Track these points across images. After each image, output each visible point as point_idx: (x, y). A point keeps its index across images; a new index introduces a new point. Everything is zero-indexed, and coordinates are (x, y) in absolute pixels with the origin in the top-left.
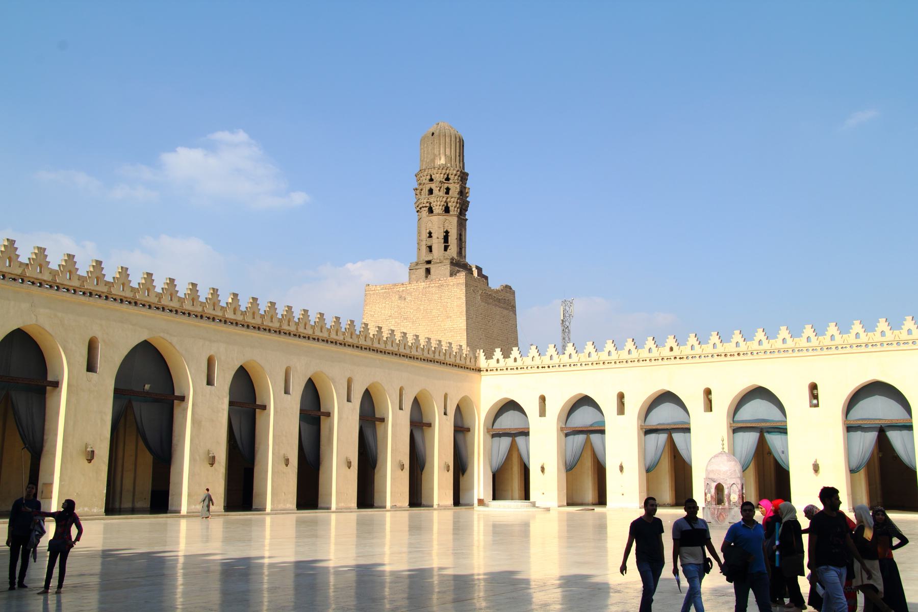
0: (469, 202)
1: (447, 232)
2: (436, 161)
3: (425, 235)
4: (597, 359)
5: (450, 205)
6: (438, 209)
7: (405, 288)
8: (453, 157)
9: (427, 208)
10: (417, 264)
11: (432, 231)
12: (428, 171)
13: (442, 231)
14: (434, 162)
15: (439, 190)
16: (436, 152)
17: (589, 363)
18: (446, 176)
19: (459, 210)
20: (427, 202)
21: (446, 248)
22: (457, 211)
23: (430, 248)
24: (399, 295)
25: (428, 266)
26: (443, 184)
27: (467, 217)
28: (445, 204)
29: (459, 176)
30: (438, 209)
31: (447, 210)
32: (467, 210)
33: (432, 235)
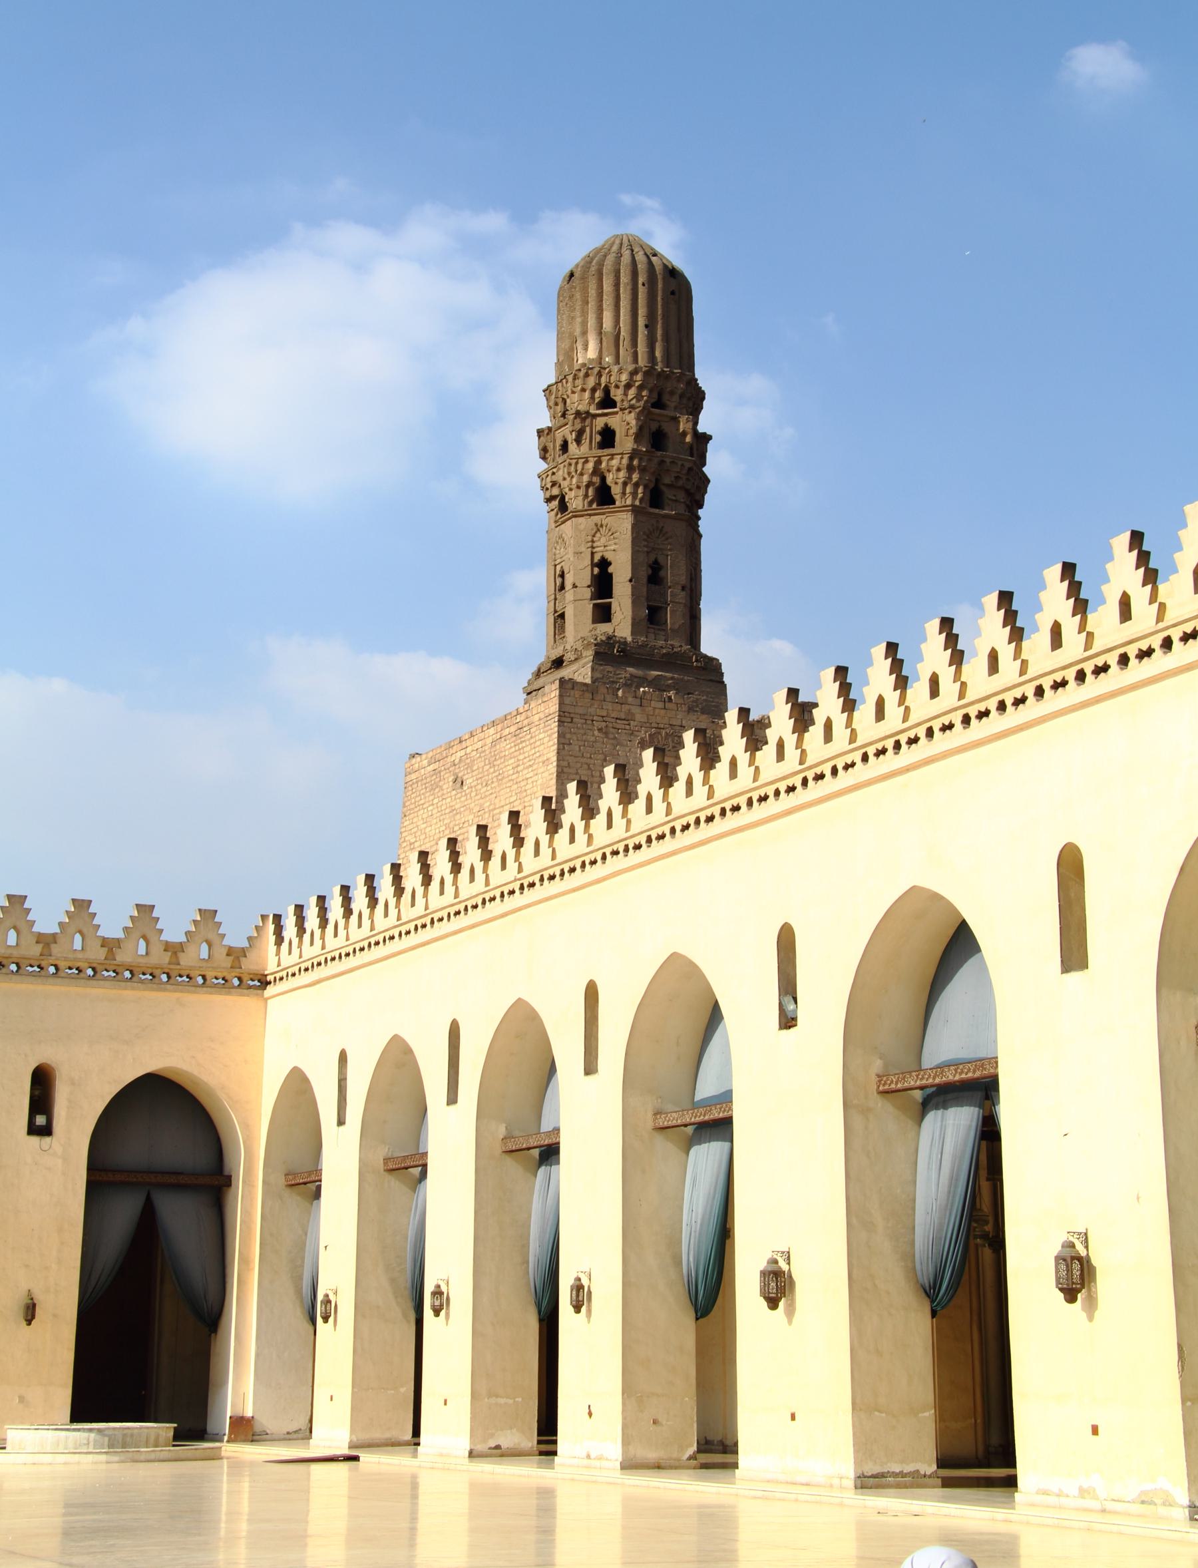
5: (610, 478)
6: (576, 501)
7: (463, 753)
8: (625, 333)
9: (555, 503)
12: (558, 390)
16: (578, 332)
18: (598, 394)
19: (640, 490)
21: (603, 614)
22: (634, 494)
24: (453, 775)
26: (588, 422)
28: (596, 480)
29: (641, 388)
30: (576, 501)
31: (604, 497)
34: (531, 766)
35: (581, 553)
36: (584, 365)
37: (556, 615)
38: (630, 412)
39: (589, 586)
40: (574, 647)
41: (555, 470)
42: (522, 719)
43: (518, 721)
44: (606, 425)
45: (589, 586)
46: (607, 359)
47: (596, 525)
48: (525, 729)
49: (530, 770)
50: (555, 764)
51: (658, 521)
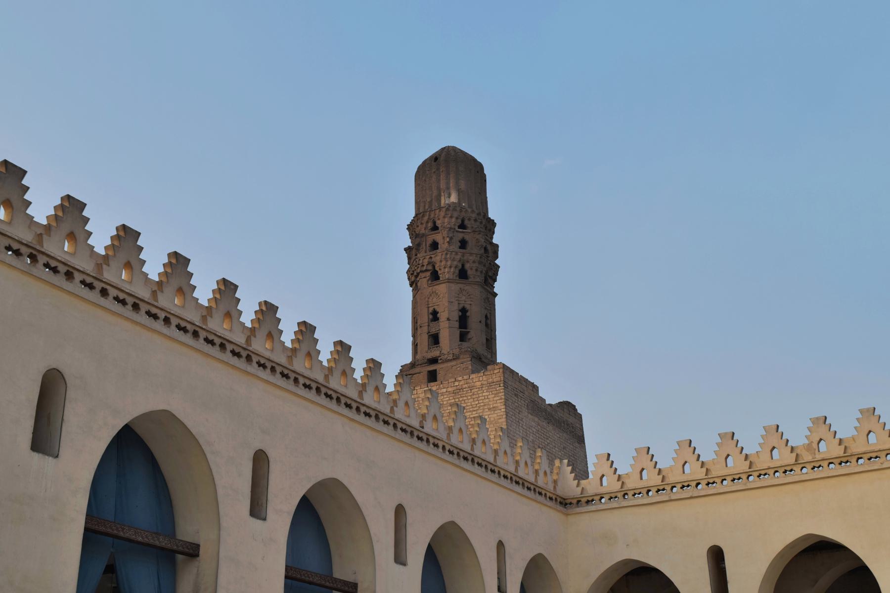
0: (499, 267)
1: (464, 311)
2: (443, 198)
3: (425, 318)
4: (841, 454)
5: (467, 266)
6: (446, 273)
9: (428, 274)
10: (413, 365)
11: (438, 310)
12: (430, 215)
13: (456, 307)
14: (440, 201)
15: (448, 242)
17: (822, 463)
18: (460, 221)
20: (429, 263)
21: (463, 337)
23: (435, 339)
25: (432, 368)
27: (495, 290)
28: (460, 266)
30: (446, 273)
31: (463, 274)
32: (495, 280)
33: (438, 315)
34: (474, 411)
35: (452, 302)
36: (449, 205)
37: (429, 334)
38: (479, 234)
39: (457, 321)
40: (451, 352)
41: (433, 256)
42: (460, 384)
43: (455, 385)
44: (463, 238)
45: (457, 321)
46: (464, 204)
47: (461, 289)
48: (465, 390)
49: (474, 413)
50: (504, 410)
51: (487, 294)
